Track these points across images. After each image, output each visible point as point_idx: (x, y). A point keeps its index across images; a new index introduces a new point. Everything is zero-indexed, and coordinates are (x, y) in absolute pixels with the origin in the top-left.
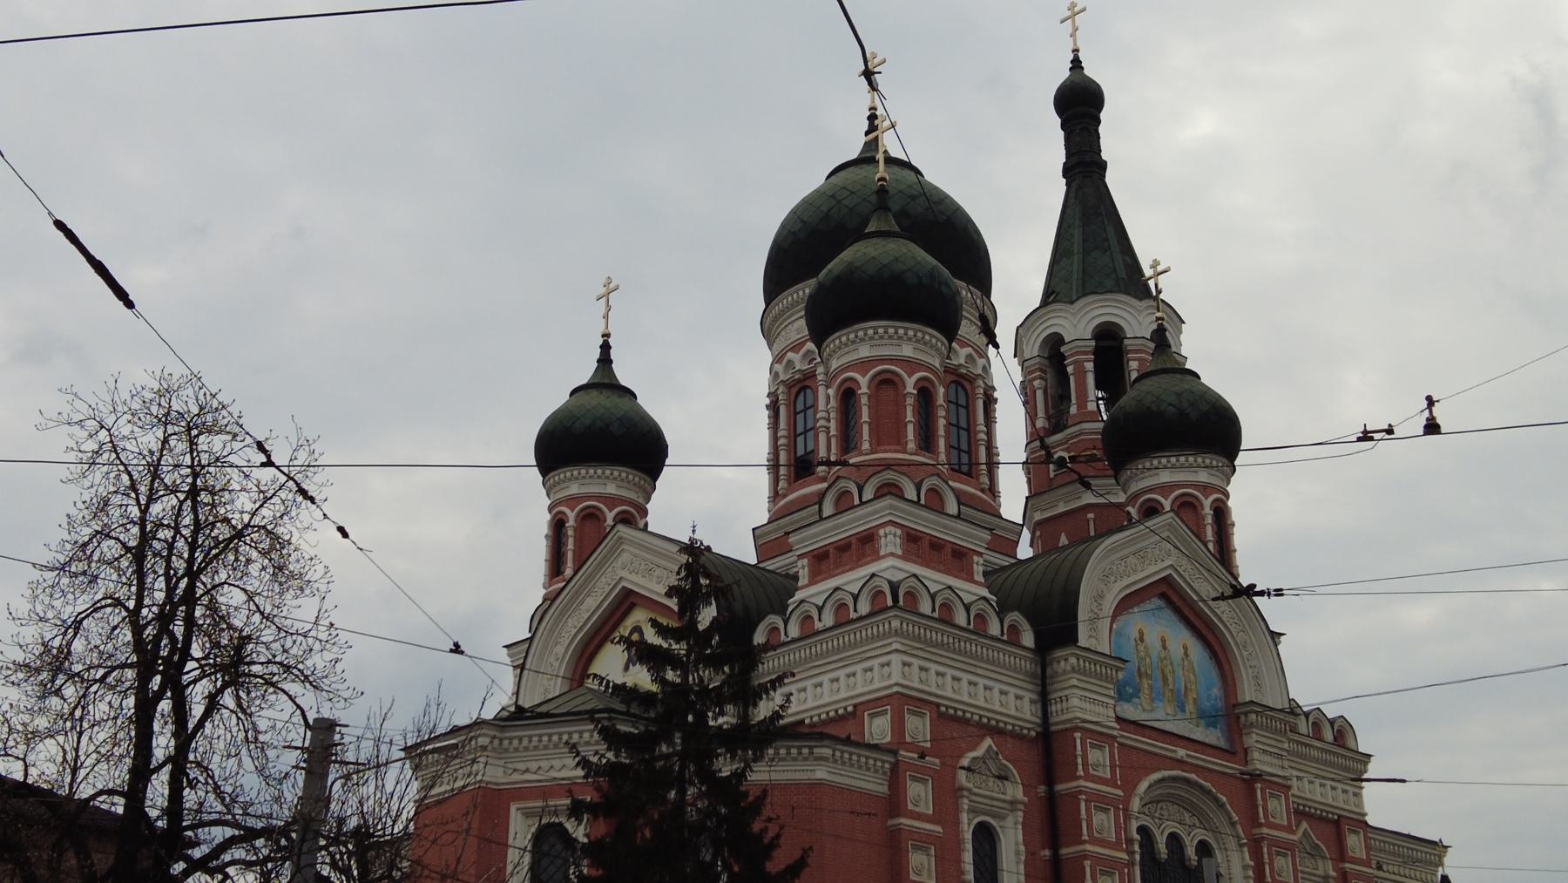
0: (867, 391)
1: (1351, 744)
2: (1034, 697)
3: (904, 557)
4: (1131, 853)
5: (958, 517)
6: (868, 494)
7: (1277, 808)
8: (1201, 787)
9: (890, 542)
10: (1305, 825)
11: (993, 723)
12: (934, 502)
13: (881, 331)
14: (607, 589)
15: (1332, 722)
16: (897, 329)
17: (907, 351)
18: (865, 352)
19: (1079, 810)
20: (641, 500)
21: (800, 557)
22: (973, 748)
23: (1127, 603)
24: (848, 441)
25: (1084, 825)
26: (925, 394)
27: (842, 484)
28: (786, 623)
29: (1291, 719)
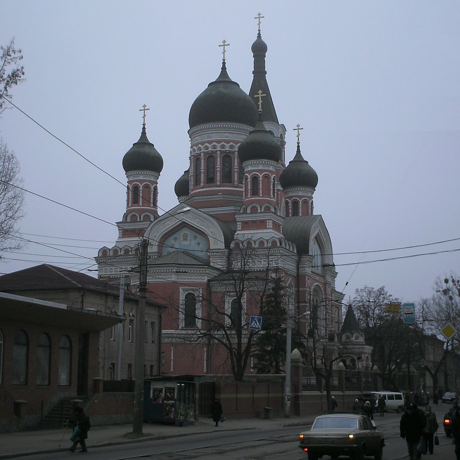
3: (272, 229)
6: (262, 210)
9: (270, 224)
18: (261, 167)
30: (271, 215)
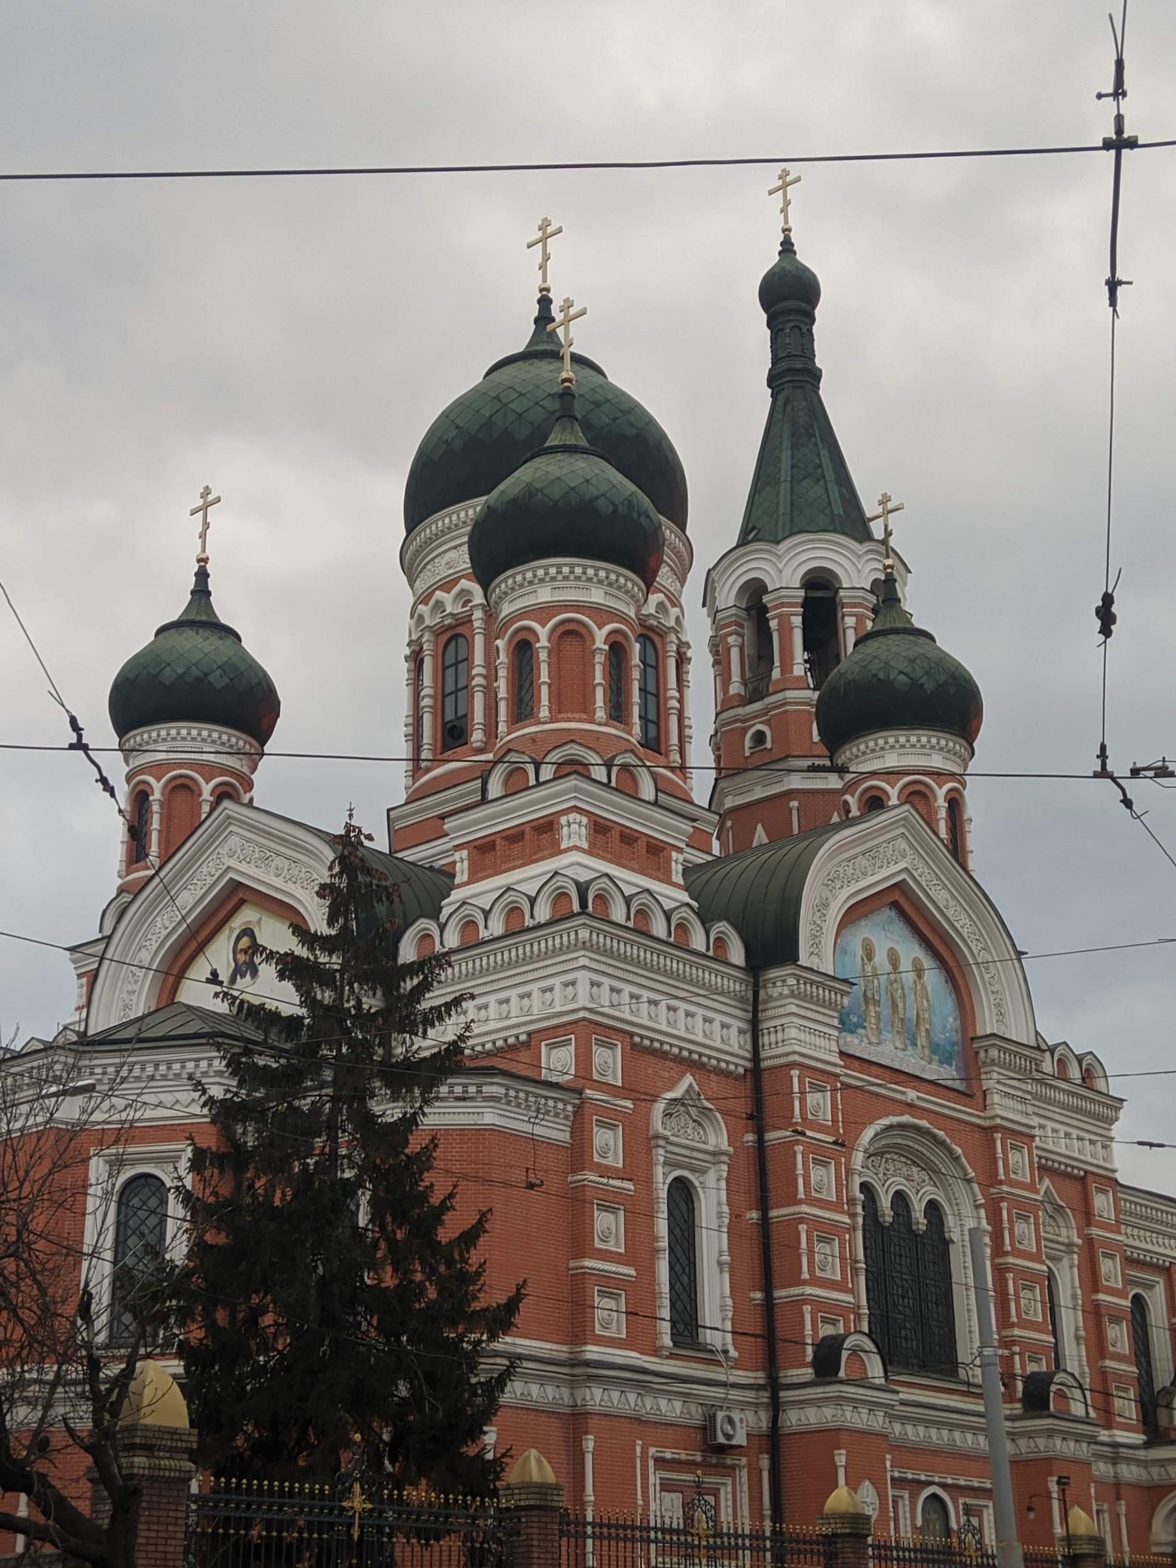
0: (546, 644)
1: (1100, 1085)
2: (744, 1025)
3: (590, 852)
4: (853, 1216)
5: (656, 803)
6: (547, 772)
7: (1019, 1162)
8: (934, 1137)
9: (574, 832)
10: (1047, 1182)
11: (695, 1057)
12: (627, 787)
13: (566, 570)
14: (210, 881)
15: (1080, 1059)
16: (585, 568)
17: (597, 596)
19: (795, 1165)
20: (246, 770)
21: (458, 848)
22: (670, 1089)
23: (856, 913)
24: (522, 710)
25: (800, 1181)
26: (617, 649)
27: (513, 757)
28: (442, 928)
29: (1036, 1055)
30: (576, 789)
